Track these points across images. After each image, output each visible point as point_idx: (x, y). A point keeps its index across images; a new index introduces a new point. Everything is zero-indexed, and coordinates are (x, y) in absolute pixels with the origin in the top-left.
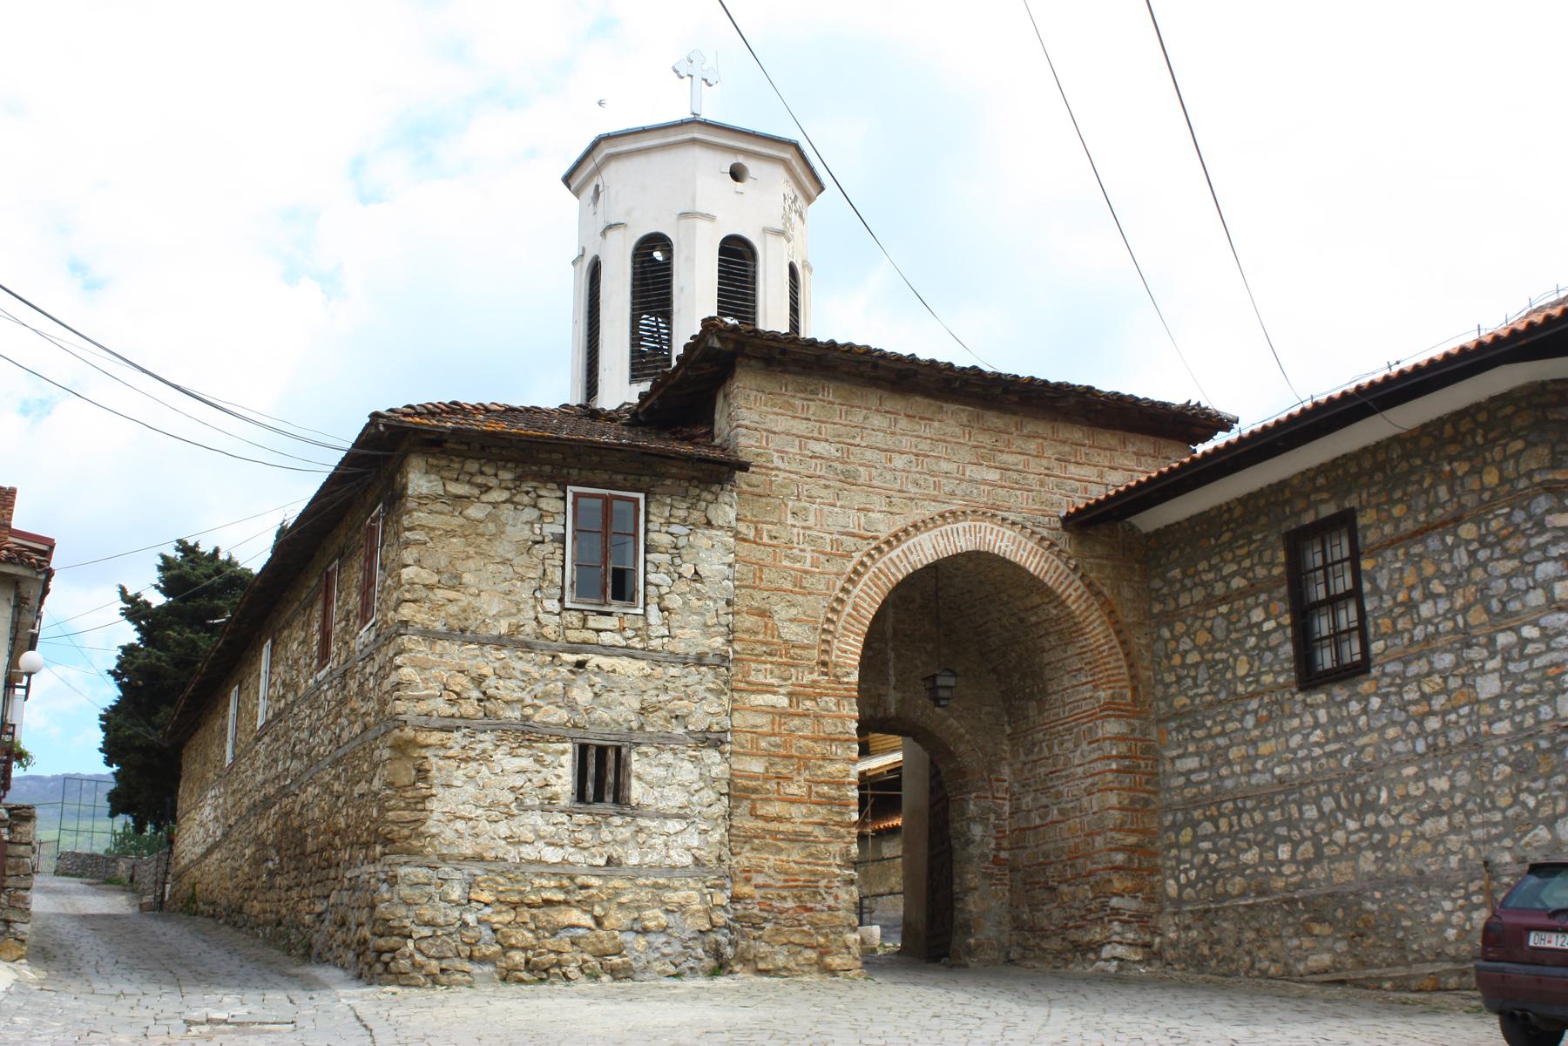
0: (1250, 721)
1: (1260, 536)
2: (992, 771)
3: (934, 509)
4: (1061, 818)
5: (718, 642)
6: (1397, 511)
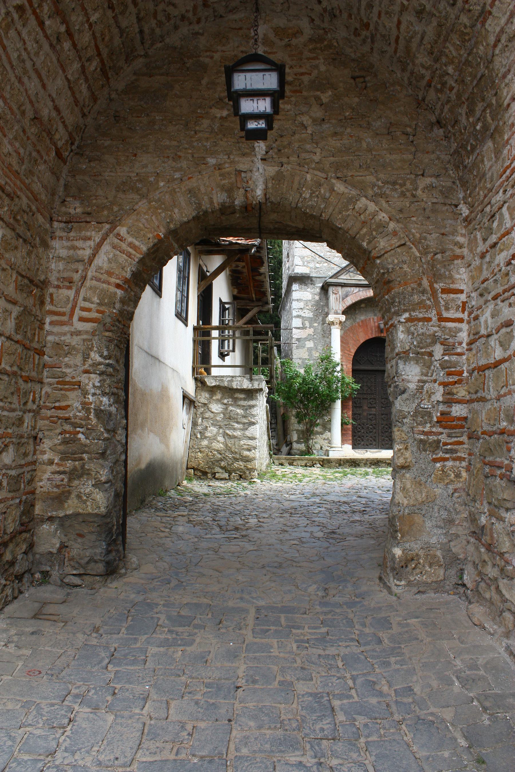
2: (436, 277)
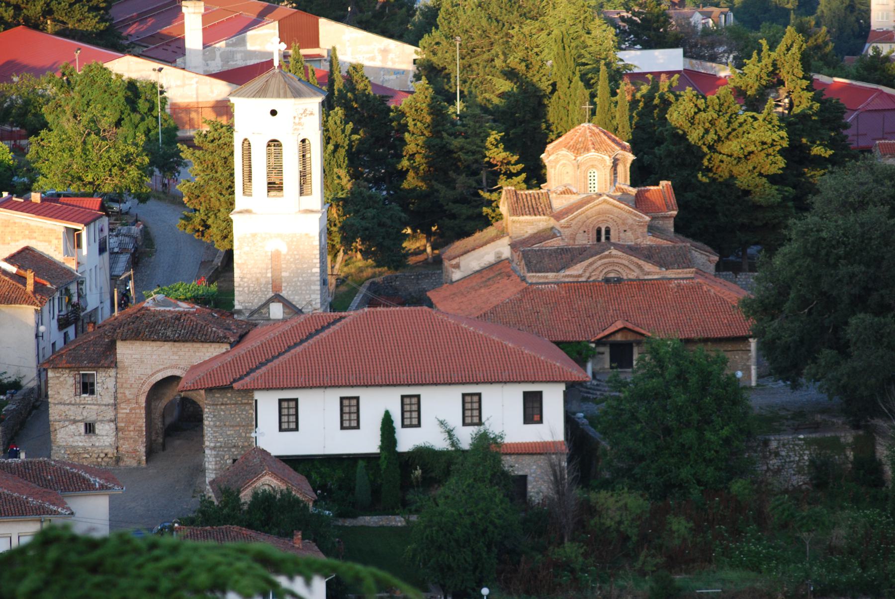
3: (161, 367)
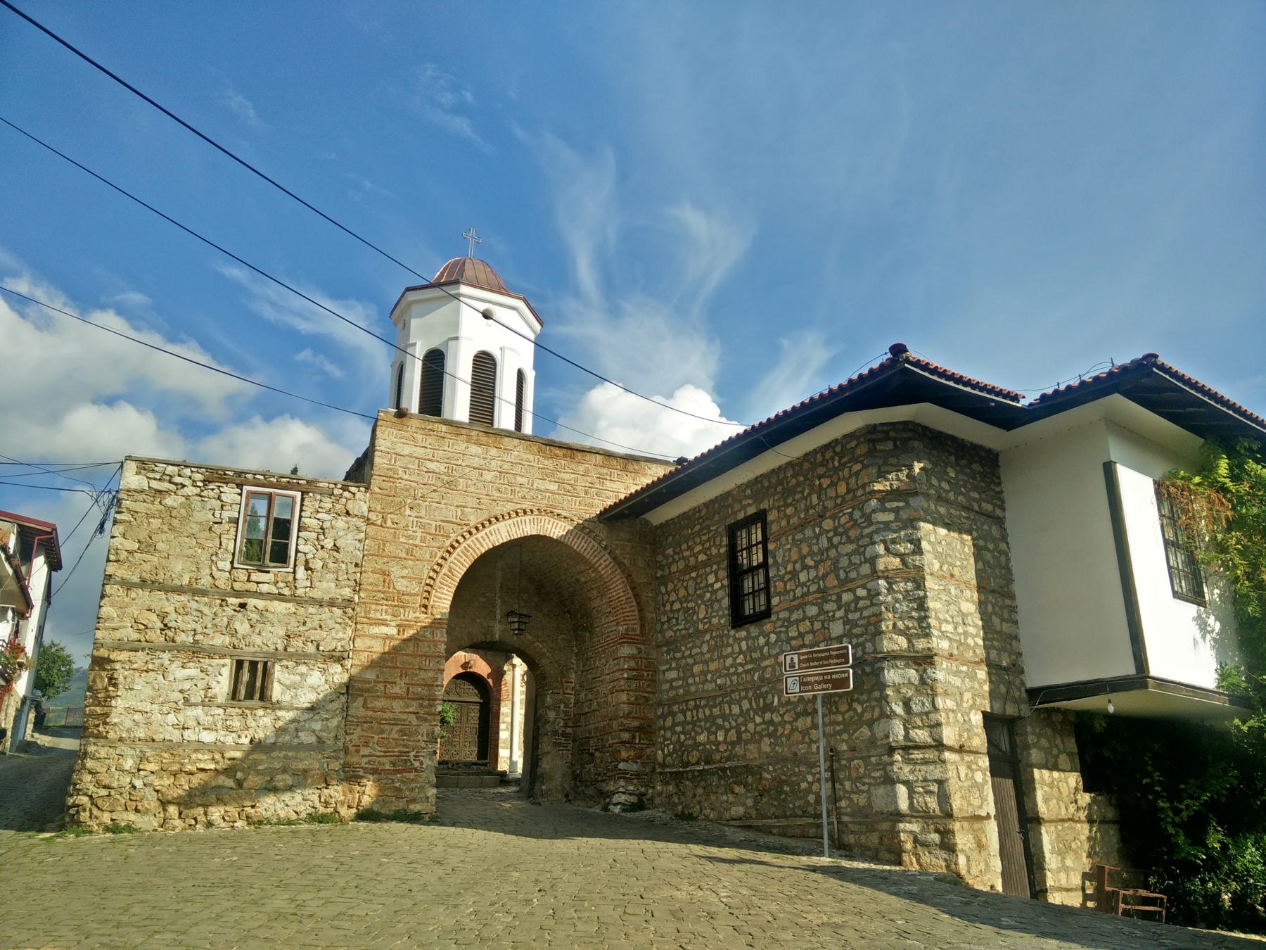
0: (705, 648)
1: (714, 528)
3: (510, 507)
4: (598, 708)
5: (347, 592)
6: (789, 511)
